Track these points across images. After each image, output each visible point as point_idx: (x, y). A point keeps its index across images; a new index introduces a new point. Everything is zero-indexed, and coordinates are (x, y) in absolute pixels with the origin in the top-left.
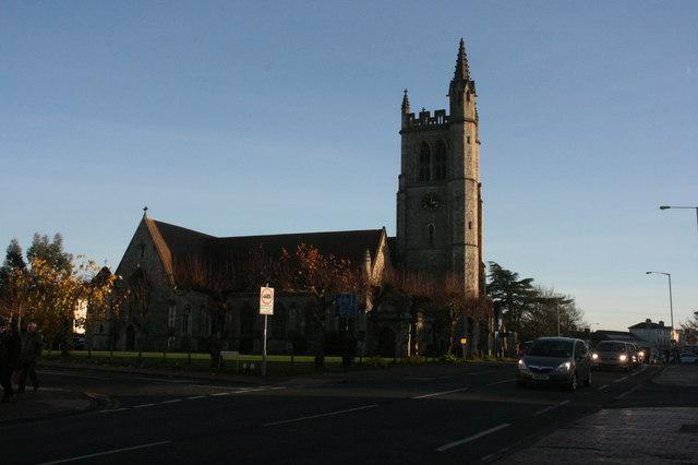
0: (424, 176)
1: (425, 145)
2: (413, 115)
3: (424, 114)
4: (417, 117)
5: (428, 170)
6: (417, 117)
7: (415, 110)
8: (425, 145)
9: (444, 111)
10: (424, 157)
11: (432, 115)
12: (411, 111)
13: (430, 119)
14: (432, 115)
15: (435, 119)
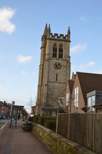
0: (54, 56)
1: (55, 45)
2: (52, 34)
3: (56, 35)
4: (53, 35)
5: (56, 55)
6: (53, 35)
7: (53, 32)
8: (55, 45)
9: (62, 35)
10: (55, 50)
11: (59, 35)
12: (51, 32)
13: (58, 37)
14: (59, 35)
15: (60, 37)
